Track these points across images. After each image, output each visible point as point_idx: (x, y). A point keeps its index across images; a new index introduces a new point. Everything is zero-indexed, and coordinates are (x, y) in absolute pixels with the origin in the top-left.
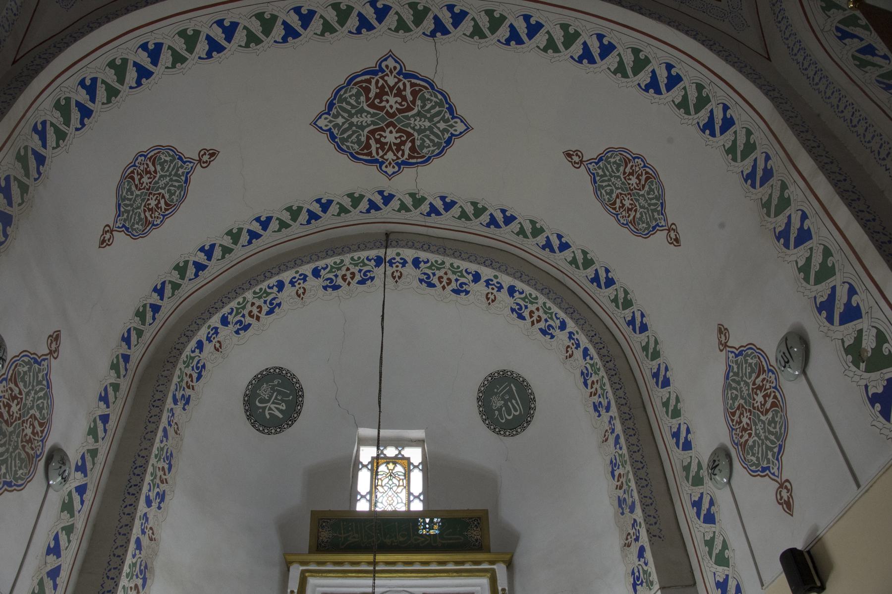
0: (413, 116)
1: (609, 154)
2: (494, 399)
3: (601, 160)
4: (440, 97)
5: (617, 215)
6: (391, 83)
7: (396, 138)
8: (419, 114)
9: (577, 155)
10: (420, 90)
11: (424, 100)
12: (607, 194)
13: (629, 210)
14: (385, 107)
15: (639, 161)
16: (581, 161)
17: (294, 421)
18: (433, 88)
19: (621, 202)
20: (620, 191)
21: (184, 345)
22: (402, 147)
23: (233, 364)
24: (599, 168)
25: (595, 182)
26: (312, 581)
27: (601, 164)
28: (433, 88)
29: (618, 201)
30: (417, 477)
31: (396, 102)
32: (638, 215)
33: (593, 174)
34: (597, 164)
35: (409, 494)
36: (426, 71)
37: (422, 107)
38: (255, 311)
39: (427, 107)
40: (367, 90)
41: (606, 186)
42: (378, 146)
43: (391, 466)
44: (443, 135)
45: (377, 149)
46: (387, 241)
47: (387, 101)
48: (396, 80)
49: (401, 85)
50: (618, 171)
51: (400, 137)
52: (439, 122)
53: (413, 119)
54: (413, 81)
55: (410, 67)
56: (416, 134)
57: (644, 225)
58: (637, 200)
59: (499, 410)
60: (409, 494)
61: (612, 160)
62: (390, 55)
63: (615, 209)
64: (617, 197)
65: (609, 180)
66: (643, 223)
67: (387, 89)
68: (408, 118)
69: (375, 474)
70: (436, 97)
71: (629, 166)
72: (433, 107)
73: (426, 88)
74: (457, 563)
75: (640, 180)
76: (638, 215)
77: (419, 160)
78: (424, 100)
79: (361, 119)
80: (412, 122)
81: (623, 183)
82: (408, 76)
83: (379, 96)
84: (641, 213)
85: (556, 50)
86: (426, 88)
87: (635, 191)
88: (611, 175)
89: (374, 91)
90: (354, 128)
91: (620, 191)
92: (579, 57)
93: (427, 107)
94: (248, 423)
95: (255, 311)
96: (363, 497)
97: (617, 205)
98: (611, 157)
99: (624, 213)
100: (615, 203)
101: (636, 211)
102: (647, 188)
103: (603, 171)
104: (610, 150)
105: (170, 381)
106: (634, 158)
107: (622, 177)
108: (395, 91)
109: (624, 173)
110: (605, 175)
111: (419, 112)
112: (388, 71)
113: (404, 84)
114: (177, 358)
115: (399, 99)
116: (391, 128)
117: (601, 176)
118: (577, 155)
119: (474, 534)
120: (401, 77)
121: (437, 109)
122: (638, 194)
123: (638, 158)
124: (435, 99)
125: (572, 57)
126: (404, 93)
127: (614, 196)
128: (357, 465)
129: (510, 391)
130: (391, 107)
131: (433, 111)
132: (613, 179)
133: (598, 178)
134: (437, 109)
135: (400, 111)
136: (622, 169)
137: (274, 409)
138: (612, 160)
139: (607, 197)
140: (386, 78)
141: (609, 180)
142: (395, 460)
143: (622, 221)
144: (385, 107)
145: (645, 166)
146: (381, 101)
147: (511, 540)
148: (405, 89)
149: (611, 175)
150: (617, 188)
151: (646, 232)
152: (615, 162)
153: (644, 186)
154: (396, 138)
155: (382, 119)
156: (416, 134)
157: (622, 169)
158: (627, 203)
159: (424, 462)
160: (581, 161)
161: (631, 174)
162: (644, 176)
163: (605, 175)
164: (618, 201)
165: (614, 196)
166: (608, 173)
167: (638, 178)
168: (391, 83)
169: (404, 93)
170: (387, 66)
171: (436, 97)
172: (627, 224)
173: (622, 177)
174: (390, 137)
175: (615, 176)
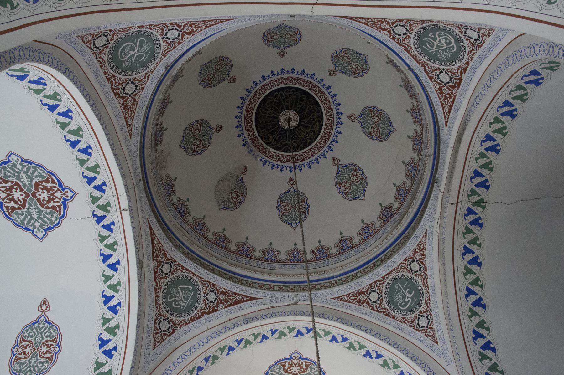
0: (38, 208)
1: (55, 328)
3: (49, 323)
4: (57, 222)
5: (17, 345)
6: (56, 194)
7: (18, 198)
8: (40, 211)
9: (47, 307)
10: (57, 211)
11: (51, 213)
12: (29, 334)
13: (24, 353)
14: (39, 191)
15: (58, 349)
16: (44, 311)
18: (61, 218)
19: (27, 345)
20: (34, 342)
22: (12, 202)
24: (44, 324)
25: (34, 324)
27: (47, 324)
28: (61, 218)
29: (27, 343)
31: (44, 198)
32: (23, 361)
33: (38, 321)
34: (46, 321)
36: (70, 213)
37: (46, 213)
39: (47, 215)
40: (47, 181)
41: (34, 332)
42: (8, 188)
44: (31, 226)
45: (6, 187)
47: (43, 193)
48: (60, 197)
49: (57, 200)
50: (47, 337)
51: (19, 200)
52: (39, 223)
53: (35, 207)
54: (62, 207)
55: (70, 205)
56: (26, 210)
57: (18, 368)
58: (33, 356)
61: (52, 331)
62: (75, 194)
63: (21, 342)
64: (30, 342)
65: (38, 333)
66: (20, 366)
67: (51, 192)
68: (35, 204)
70: (56, 220)
71: (52, 343)
72: (48, 219)
73: (60, 214)
75: (46, 353)
76: (23, 361)
77: (7, 213)
78: (51, 213)
79: (25, 178)
80: (33, 207)
81: (40, 343)
82: (64, 204)
83: (45, 188)
84: (25, 362)
85: (105, 282)
86: (60, 214)
87: (38, 352)
88: (42, 333)
89: (49, 185)
90: (16, 174)
91: (34, 342)
92: (105, 295)
93: (47, 215)
97: (24, 343)
98: (53, 329)
99: (20, 350)
100: (25, 341)
101: (25, 358)
102: (43, 360)
103: (43, 327)
104: (58, 328)
106: (58, 345)
107: (44, 341)
108: (52, 197)
109: (47, 341)
110: (40, 329)
111: (42, 211)
112: (64, 192)
113: (58, 202)
115: (47, 199)
116: (24, 195)
117: (39, 327)
118: (47, 307)
120: (62, 200)
121: (48, 221)
122: (37, 355)
123: (59, 348)
124: (54, 219)
125: (104, 291)
126: (52, 202)
127: (29, 339)
130: (40, 195)
131: (45, 219)
132: (40, 335)
133: (36, 325)
134: (48, 221)
135: (39, 200)
136: (48, 339)
138: (52, 331)
139: (26, 334)
140: (59, 192)
141: (38, 333)
143: (15, 350)
144: (39, 191)
145: (56, 354)
146: (42, 189)
148: (54, 202)
149: (42, 333)
150: (35, 339)
151: (15, 372)
152: (51, 333)
153: (43, 357)
154: (18, 198)
155: (29, 190)
156: (26, 210)
157: (48, 339)
158: (28, 350)
160: (44, 311)
161: (48, 346)
162: (49, 355)
163: (40, 329)
164: (27, 343)
165: (29, 339)
166: (42, 330)
167: (47, 351)
168: (56, 194)
169: (52, 202)
170: (67, 192)
171: (56, 220)
172: (14, 355)
173: (44, 341)
174: (17, 195)
175: (42, 336)
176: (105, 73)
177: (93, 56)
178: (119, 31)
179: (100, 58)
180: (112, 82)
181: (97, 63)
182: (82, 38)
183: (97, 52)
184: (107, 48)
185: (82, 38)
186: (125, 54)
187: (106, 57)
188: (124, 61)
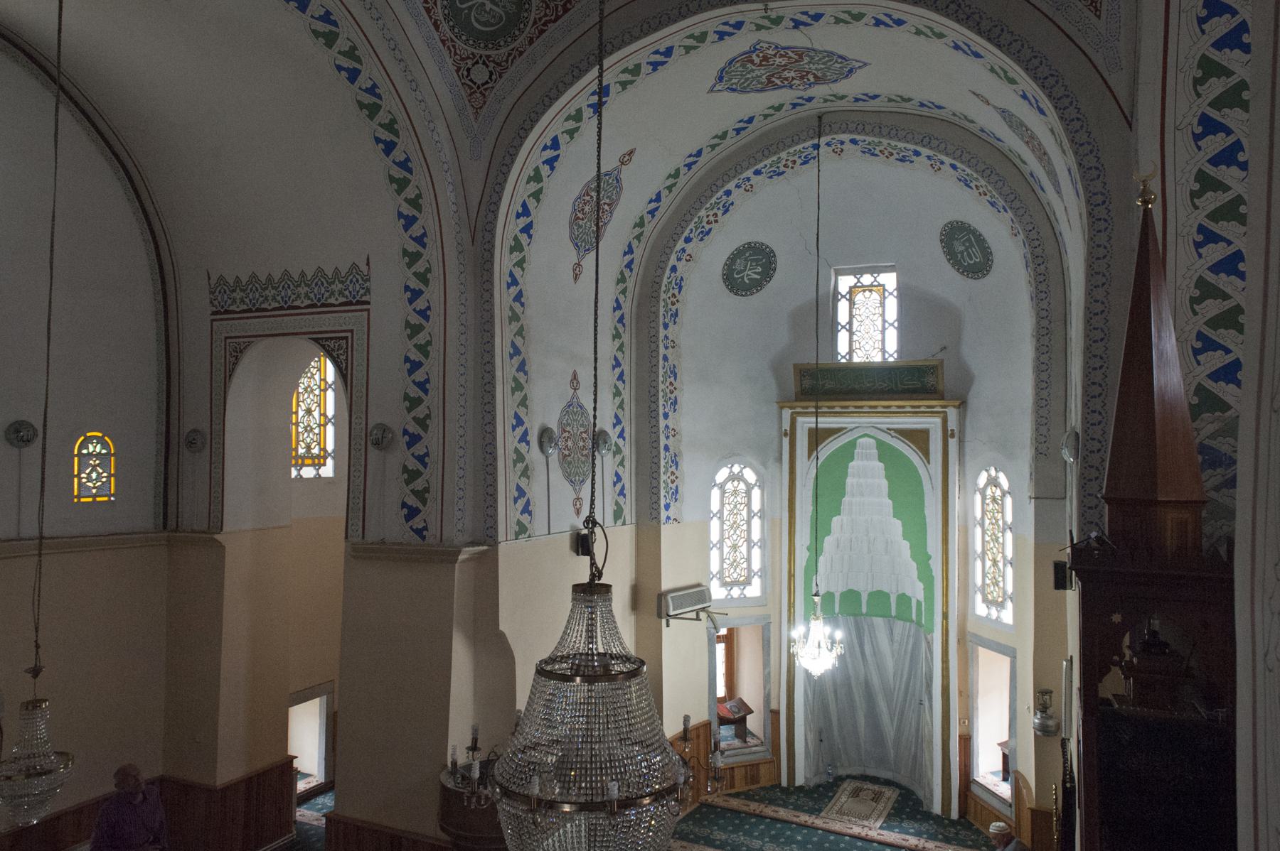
2: (956, 244)
17: (771, 277)
21: (661, 276)
23: (706, 261)
26: (800, 419)
30: (892, 305)
35: (884, 321)
38: (712, 219)
43: (867, 293)
46: (820, 126)
59: (962, 253)
60: (884, 321)
69: (852, 303)
74: (913, 407)
94: (732, 295)
95: (712, 219)
96: (843, 327)
105: (657, 317)
114: (658, 291)
119: (930, 380)
128: (836, 296)
129: (969, 240)
137: (752, 274)
142: (870, 288)
147: (967, 379)
159: (899, 288)
176: (531, 42)
177: (505, 76)
178: (456, 54)
179: (507, 61)
180: (545, 24)
181: (517, 62)
182: (477, 110)
183: (498, 69)
184: (488, 57)
185: (477, 110)
186: (494, 17)
187: (504, 51)
188: (506, 13)
